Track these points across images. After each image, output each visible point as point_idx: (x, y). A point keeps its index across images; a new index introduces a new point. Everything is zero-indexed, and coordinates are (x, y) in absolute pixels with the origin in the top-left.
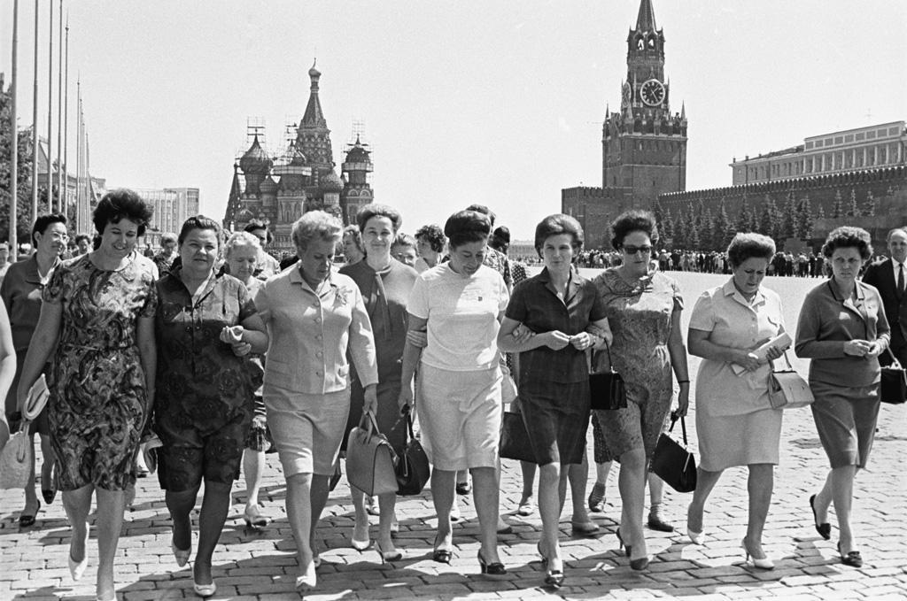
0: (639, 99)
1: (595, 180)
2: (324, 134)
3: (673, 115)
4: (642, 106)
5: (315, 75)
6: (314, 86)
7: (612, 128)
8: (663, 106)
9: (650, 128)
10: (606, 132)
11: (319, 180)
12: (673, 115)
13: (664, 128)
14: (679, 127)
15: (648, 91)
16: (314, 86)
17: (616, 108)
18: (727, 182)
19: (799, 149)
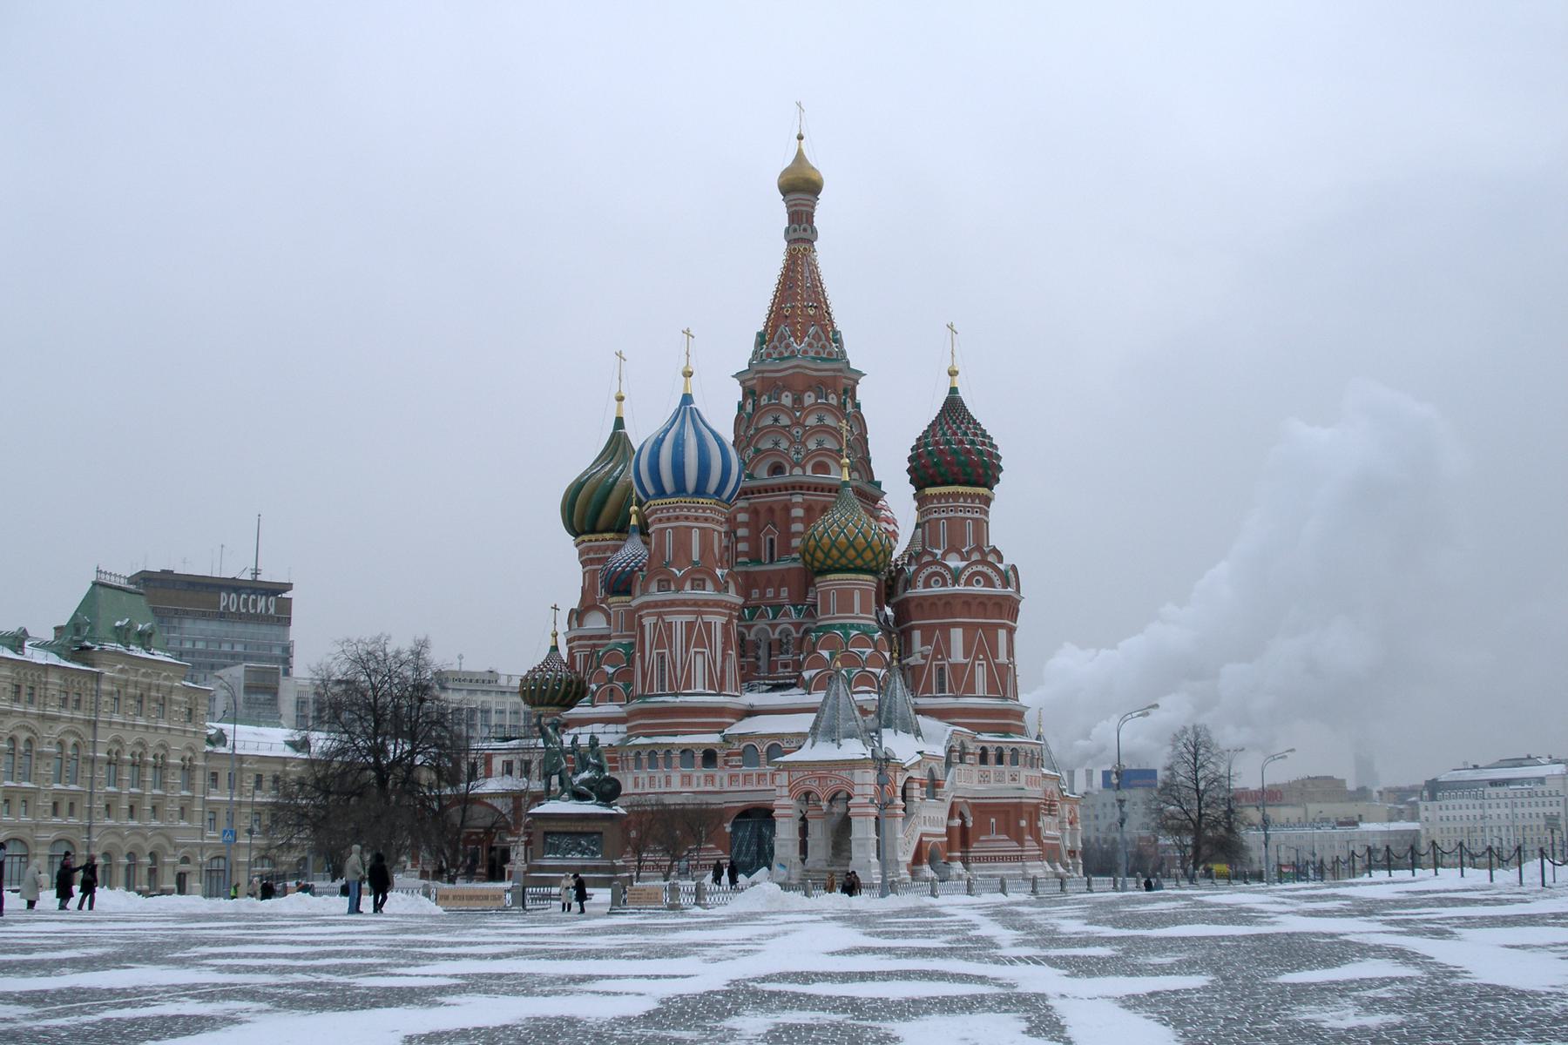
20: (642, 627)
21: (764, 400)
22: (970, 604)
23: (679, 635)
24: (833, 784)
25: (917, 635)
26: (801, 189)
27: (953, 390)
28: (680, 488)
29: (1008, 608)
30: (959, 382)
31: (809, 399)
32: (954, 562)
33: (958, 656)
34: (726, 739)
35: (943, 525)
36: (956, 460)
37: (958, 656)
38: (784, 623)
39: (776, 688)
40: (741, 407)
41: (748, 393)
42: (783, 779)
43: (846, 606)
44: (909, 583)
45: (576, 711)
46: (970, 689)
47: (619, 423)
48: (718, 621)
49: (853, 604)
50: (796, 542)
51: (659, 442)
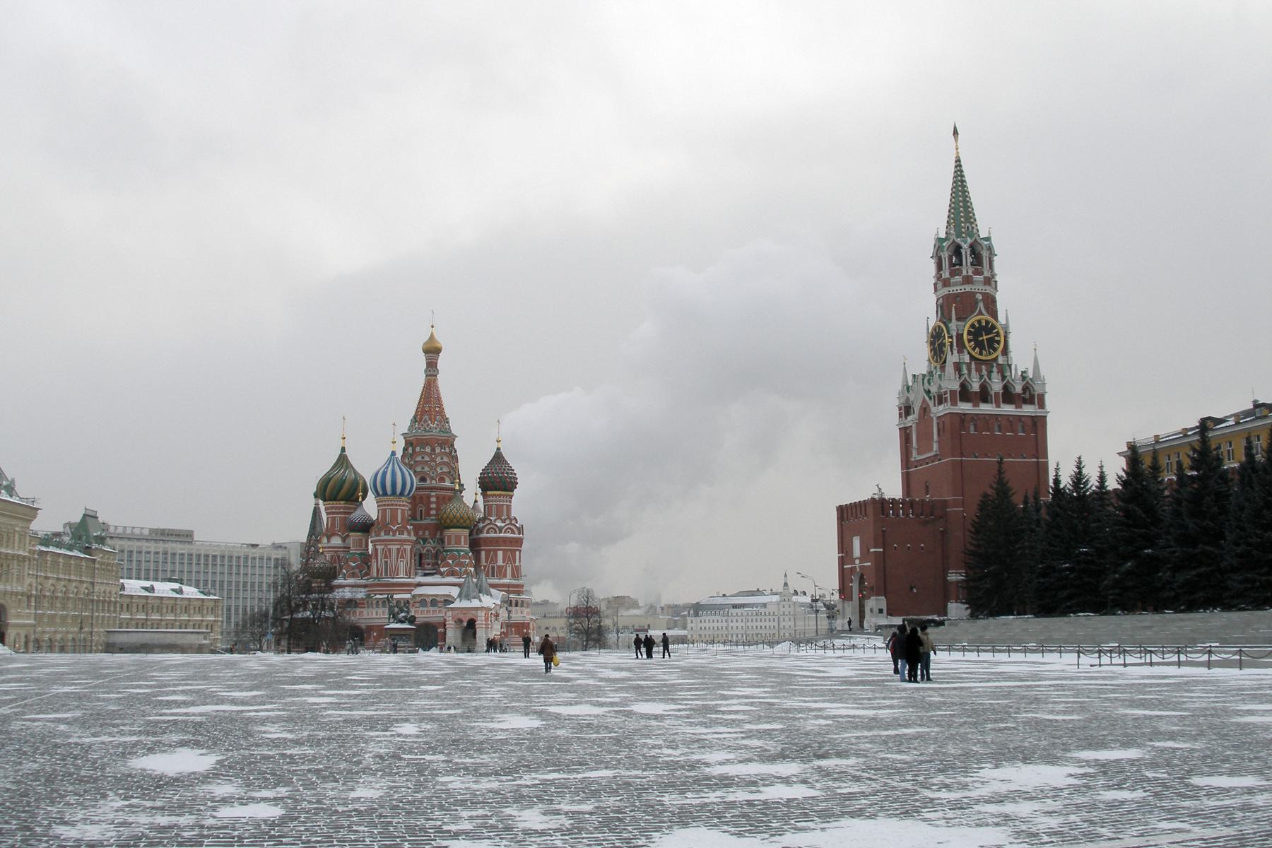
0: (961, 347)
1: (894, 489)
4: (967, 358)
6: (432, 367)
8: (1001, 360)
9: (984, 396)
10: (906, 410)
11: (438, 509)
12: (1015, 374)
13: (1008, 396)
14: (1030, 394)
20: (376, 550)
21: (418, 449)
22: (505, 541)
23: (394, 553)
24: (469, 616)
25: (483, 553)
26: (432, 351)
27: (498, 449)
28: (394, 493)
29: (519, 542)
30: (500, 445)
31: (438, 450)
32: (499, 524)
33: (500, 562)
34: (414, 596)
35: (494, 508)
36: (498, 480)
37: (500, 562)
38: (428, 546)
39: (426, 575)
40: (405, 449)
41: (409, 443)
42: (449, 614)
43: (458, 542)
44: (481, 531)
45: (336, 582)
46: (505, 576)
47: (343, 449)
48: (408, 548)
49: (459, 541)
50: (433, 512)
51: (385, 473)
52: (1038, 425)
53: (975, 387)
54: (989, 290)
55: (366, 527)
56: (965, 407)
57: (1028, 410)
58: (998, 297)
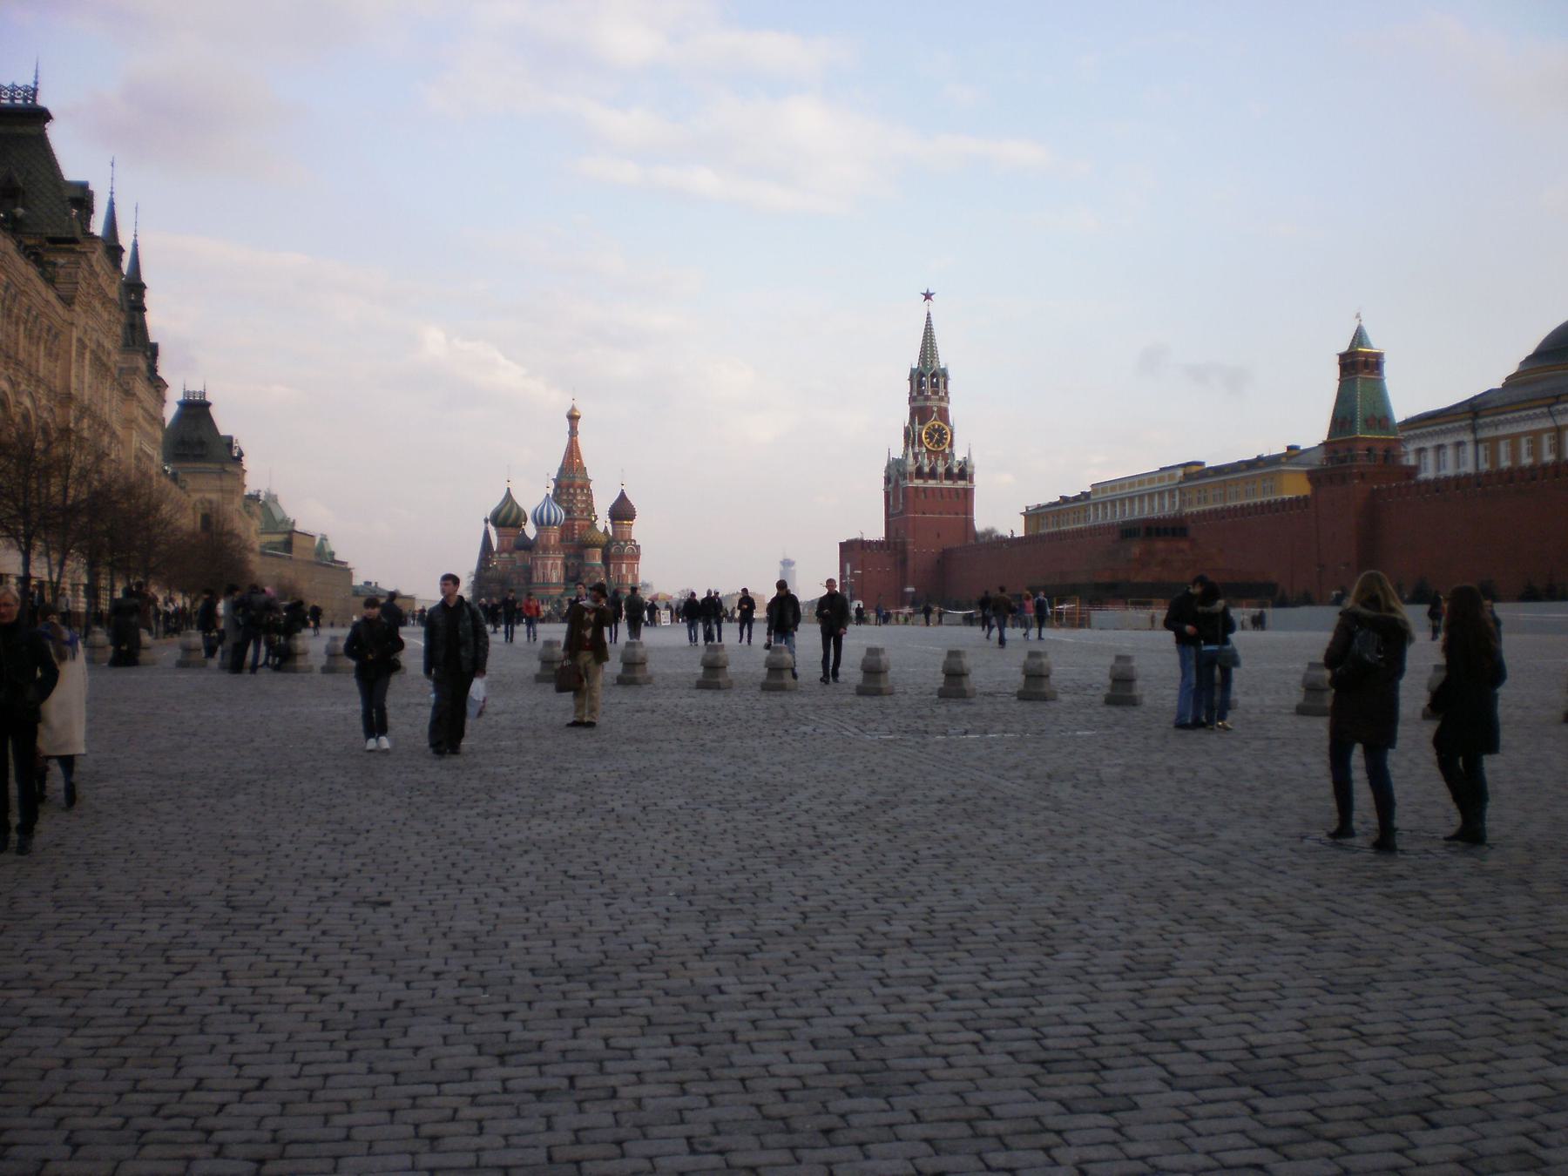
0: (921, 443)
1: (875, 530)
2: (585, 486)
3: (959, 456)
5: (573, 418)
6: (573, 432)
7: (895, 475)
9: (933, 474)
10: (888, 480)
12: (959, 456)
13: (949, 474)
14: (964, 473)
15: (930, 436)
16: (573, 432)
17: (898, 453)
18: (1020, 532)
19: (1085, 495)
36: (622, 511)
52: (967, 494)
53: (926, 469)
54: (943, 404)
55: (526, 546)
56: (918, 483)
57: (961, 484)
58: (950, 408)
